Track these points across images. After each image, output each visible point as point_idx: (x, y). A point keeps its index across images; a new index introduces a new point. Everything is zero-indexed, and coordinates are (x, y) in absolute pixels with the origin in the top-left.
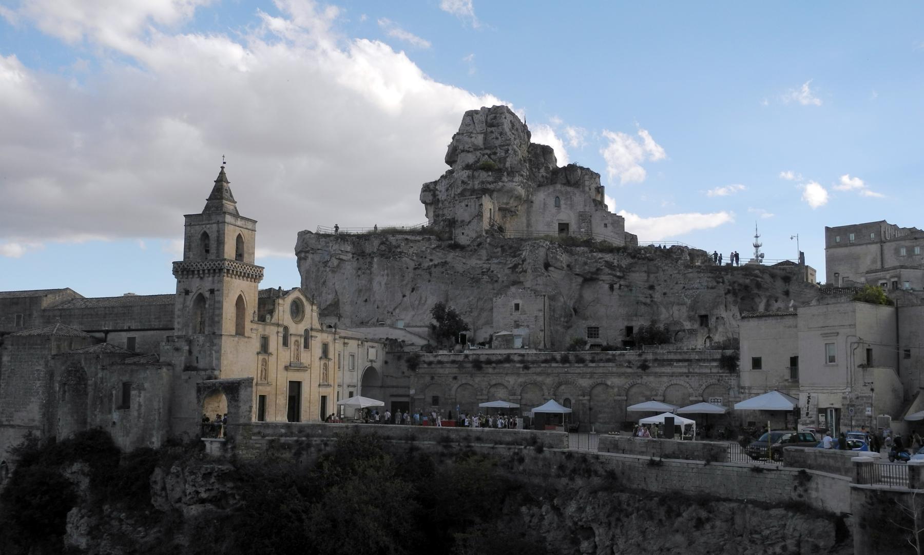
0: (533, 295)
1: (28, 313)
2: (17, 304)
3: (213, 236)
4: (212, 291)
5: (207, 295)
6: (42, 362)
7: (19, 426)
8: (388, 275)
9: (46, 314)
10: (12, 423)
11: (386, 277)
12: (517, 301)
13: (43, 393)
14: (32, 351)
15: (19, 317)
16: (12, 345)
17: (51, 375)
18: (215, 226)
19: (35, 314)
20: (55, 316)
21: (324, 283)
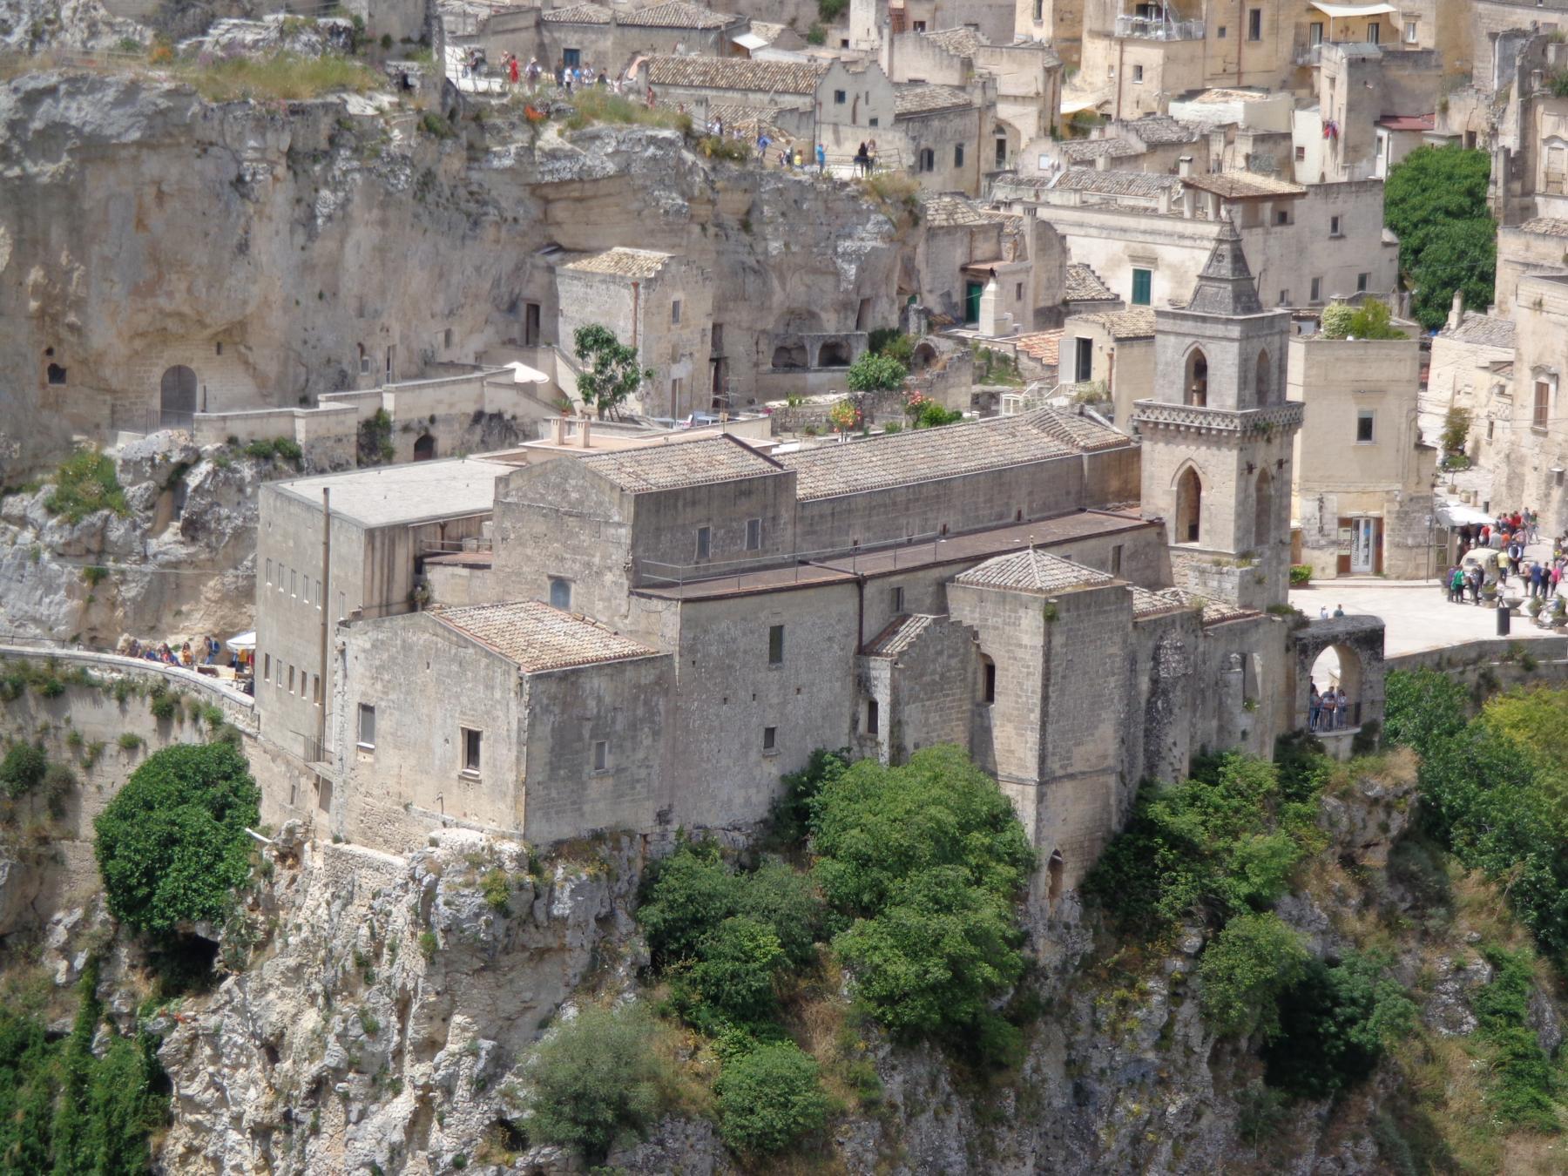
0: (700, 278)
1: (770, 514)
2: (748, 493)
3: (1274, 358)
4: (1280, 464)
5: (1274, 470)
6: (1117, 638)
7: (1083, 773)
8: (384, 223)
9: (807, 513)
10: (1070, 770)
11: (375, 233)
12: (678, 295)
13: (1121, 699)
14: (1101, 619)
15: (753, 525)
16: (1068, 610)
17: (1133, 661)
18: (1277, 338)
19: (785, 516)
20: (822, 516)
21: (243, 248)
